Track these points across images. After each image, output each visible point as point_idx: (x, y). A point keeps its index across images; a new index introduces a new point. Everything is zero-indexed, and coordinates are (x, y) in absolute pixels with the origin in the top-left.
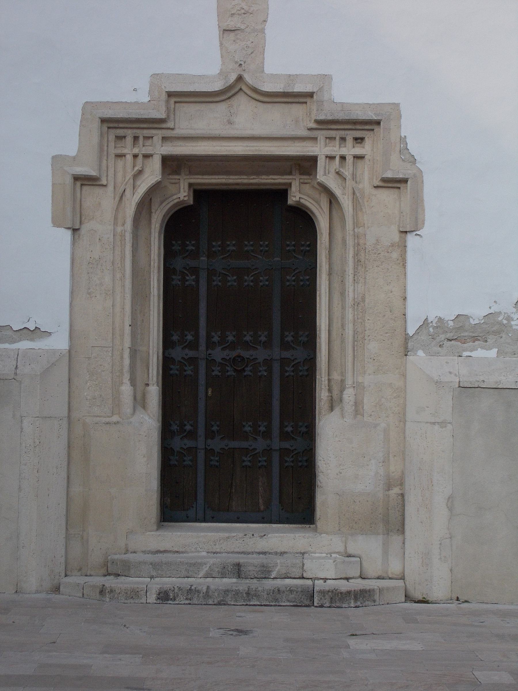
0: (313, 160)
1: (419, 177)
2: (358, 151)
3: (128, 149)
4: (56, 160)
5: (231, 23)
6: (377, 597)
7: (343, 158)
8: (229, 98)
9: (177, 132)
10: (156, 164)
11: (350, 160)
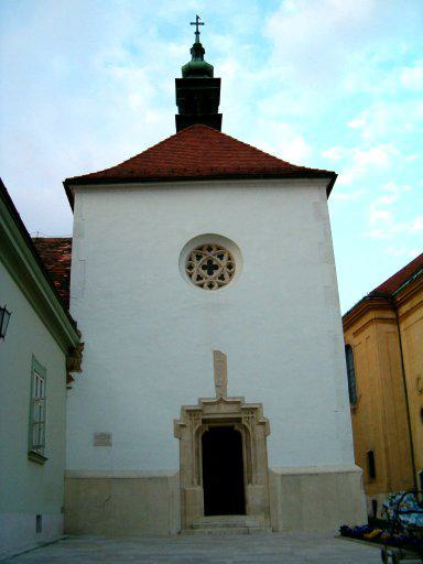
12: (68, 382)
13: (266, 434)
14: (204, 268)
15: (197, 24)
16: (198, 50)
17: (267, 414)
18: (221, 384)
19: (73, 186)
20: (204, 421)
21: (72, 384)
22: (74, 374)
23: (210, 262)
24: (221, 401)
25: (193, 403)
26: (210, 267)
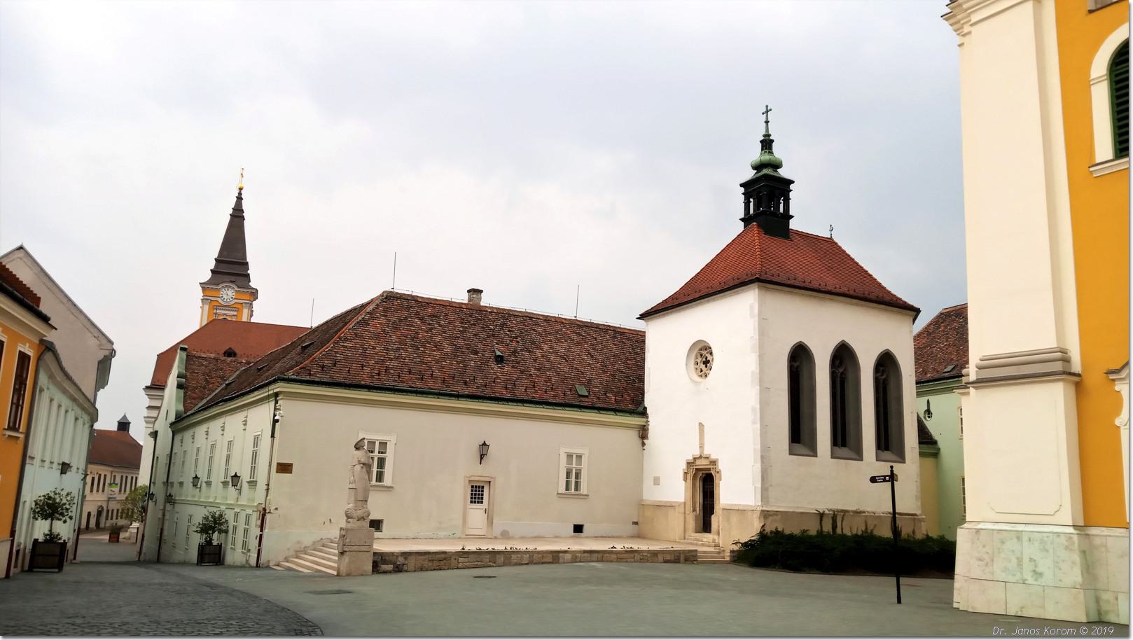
12: (643, 446)
14: (704, 363)
15: (767, 112)
16: (767, 144)
17: (721, 466)
18: (701, 447)
23: (706, 358)
24: (701, 457)
25: (690, 458)
26: (706, 362)
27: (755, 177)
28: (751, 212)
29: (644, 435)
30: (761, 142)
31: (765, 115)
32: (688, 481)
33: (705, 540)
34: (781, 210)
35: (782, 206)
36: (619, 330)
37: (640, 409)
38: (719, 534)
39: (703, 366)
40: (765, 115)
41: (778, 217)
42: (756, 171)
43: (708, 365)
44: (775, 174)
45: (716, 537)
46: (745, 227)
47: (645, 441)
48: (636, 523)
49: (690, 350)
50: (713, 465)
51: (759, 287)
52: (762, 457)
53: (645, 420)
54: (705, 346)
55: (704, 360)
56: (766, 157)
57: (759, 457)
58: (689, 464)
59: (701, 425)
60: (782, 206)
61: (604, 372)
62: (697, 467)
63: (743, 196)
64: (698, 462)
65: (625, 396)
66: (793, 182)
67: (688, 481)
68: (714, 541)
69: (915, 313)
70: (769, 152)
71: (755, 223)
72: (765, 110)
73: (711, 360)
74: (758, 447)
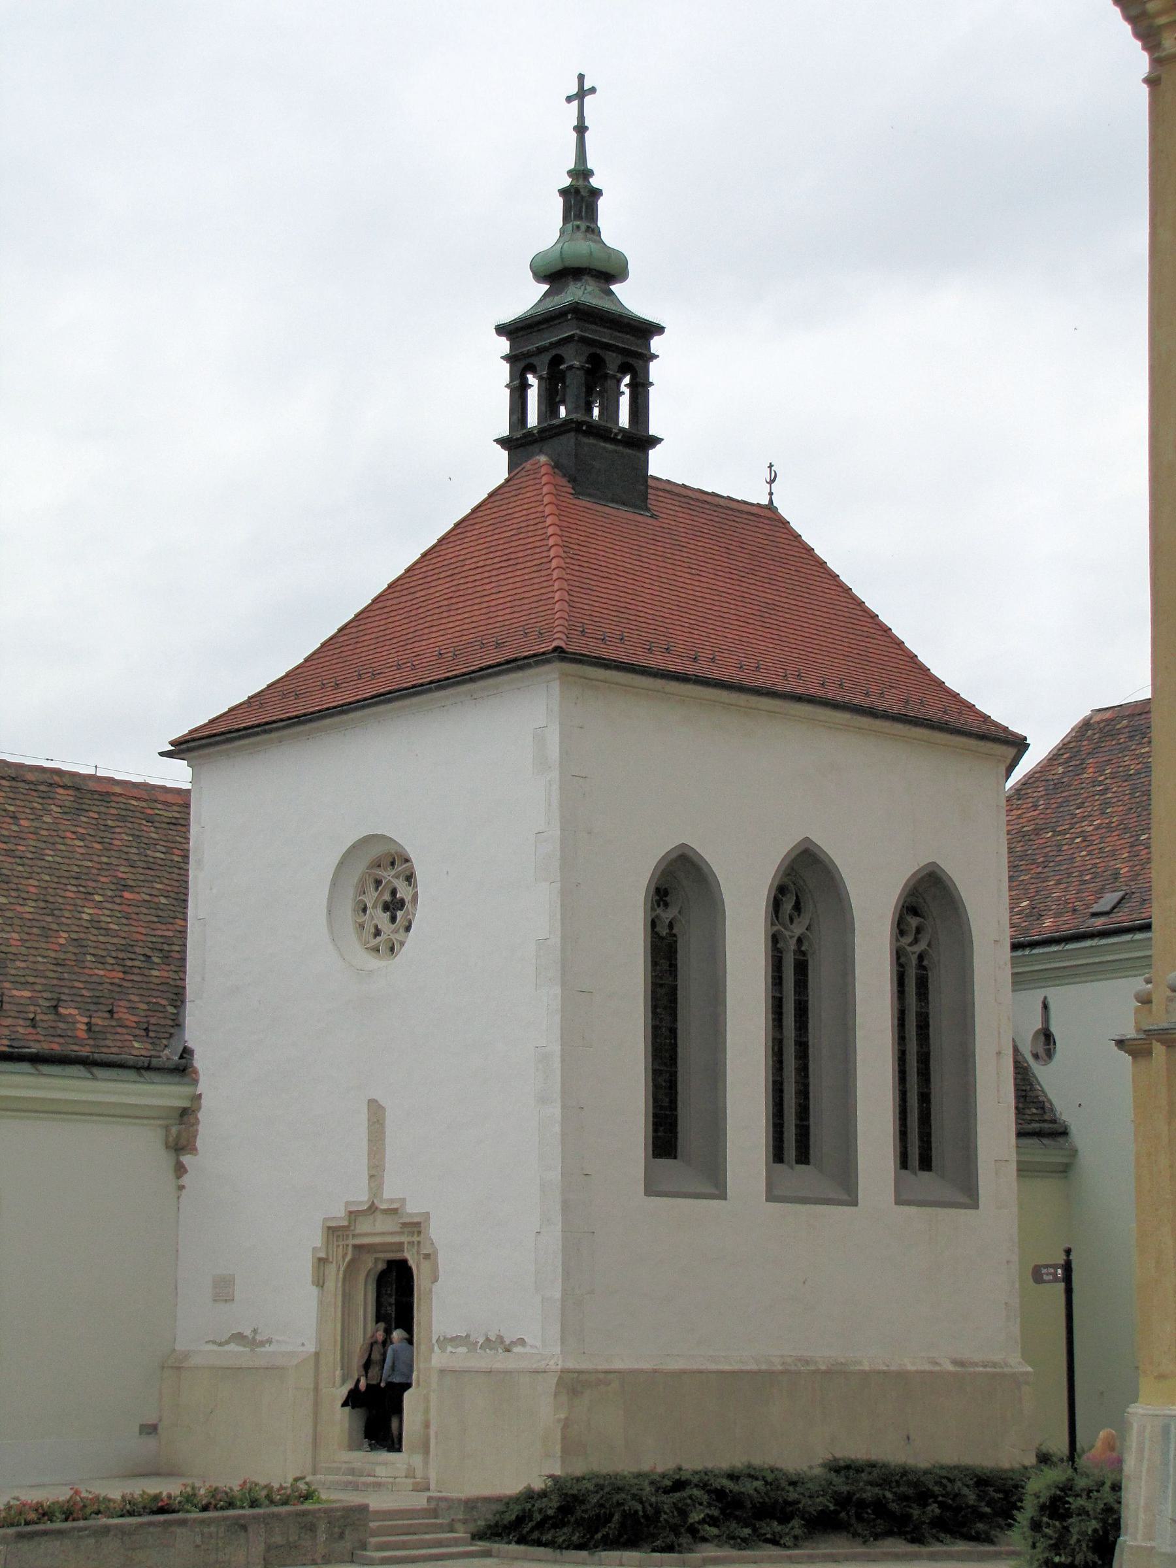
0: (402, 1244)
1: (436, 1252)
2: (418, 1239)
3: (341, 1243)
4: (314, 1249)
5: (373, 1172)
6: (390, 1487)
7: (413, 1242)
8: (374, 1211)
9: (357, 1231)
10: (350, 1249)
11: (416, 1242)
12: (179, 1177)
13: (435, 1279)
14: (386, 908)
15: (581, 94)
18: (376, 1175)
19: (182, 748)
20: (358, 1248)
21: (185, 1180)
22: (186, 1159)
23: (394, 892)
24: (372, 1209)
25: (338, 1213)
26: (394, 906)
27: (541, 309)
28: (532, 420)
29: (183, 1142)
30: (564, 192)
31: (575, 103)
32: (331, 1284)
33: (381, 1471)
34: (624, 420)
35: (624, 402)
36: (92, 785)
37: (170, 1055)
38: (426, 1450)
39: (383, 919)
40: (575, 103)
41: (614, 441)
42: (546, 287)
43: (399, 914)
44: (603, 303)
45: (417, 1460)
46: (510, 470)
47: (186, 1159)
48: (150, 1429)
49: (342, 863)
50: (412, 1233)
51: (564, 675)
52: (566, 1206)
53: (185, 1090)
54: (389, 854)
55: (387, 897)
56: (581, 247)
57: (558, 1207)
58: (333, 1232)
59: (376, 1111)
60: (624, 402)
61: (47, 933)
62: (358, 1241)
63: (506, 367)
64: (364, 1226)
65: (122, 1013)
66: (659, 329)
67: (331, 1284)
68: (410, 1474)
69: (1011, 752)
70: (588, 227)
71: (543, 459)
72: (574, 90)
73: (408, 899)
74: (555, 1175)
